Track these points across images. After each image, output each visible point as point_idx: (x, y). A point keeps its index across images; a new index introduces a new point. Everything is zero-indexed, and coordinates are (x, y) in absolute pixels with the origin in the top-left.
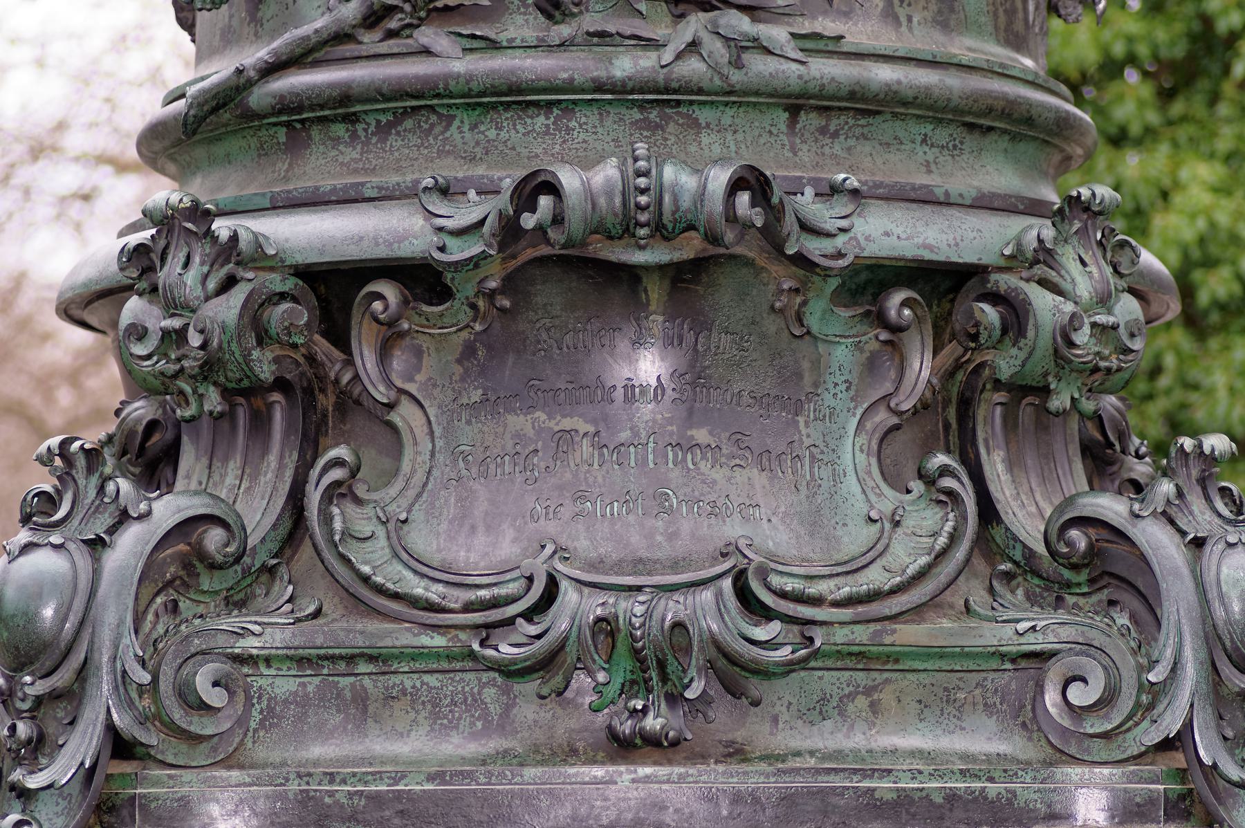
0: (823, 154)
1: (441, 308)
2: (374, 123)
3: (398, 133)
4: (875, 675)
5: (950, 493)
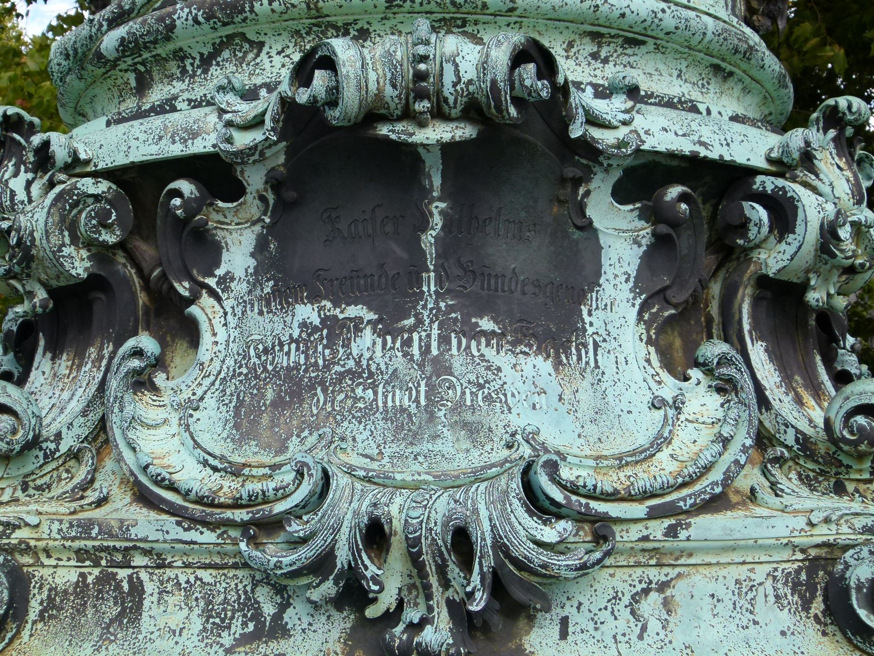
0: (596, 76)
1: (235, 204)
2: (198, 57)
3: (218, 64)
4: (666, 570)
5: (730, 380)
